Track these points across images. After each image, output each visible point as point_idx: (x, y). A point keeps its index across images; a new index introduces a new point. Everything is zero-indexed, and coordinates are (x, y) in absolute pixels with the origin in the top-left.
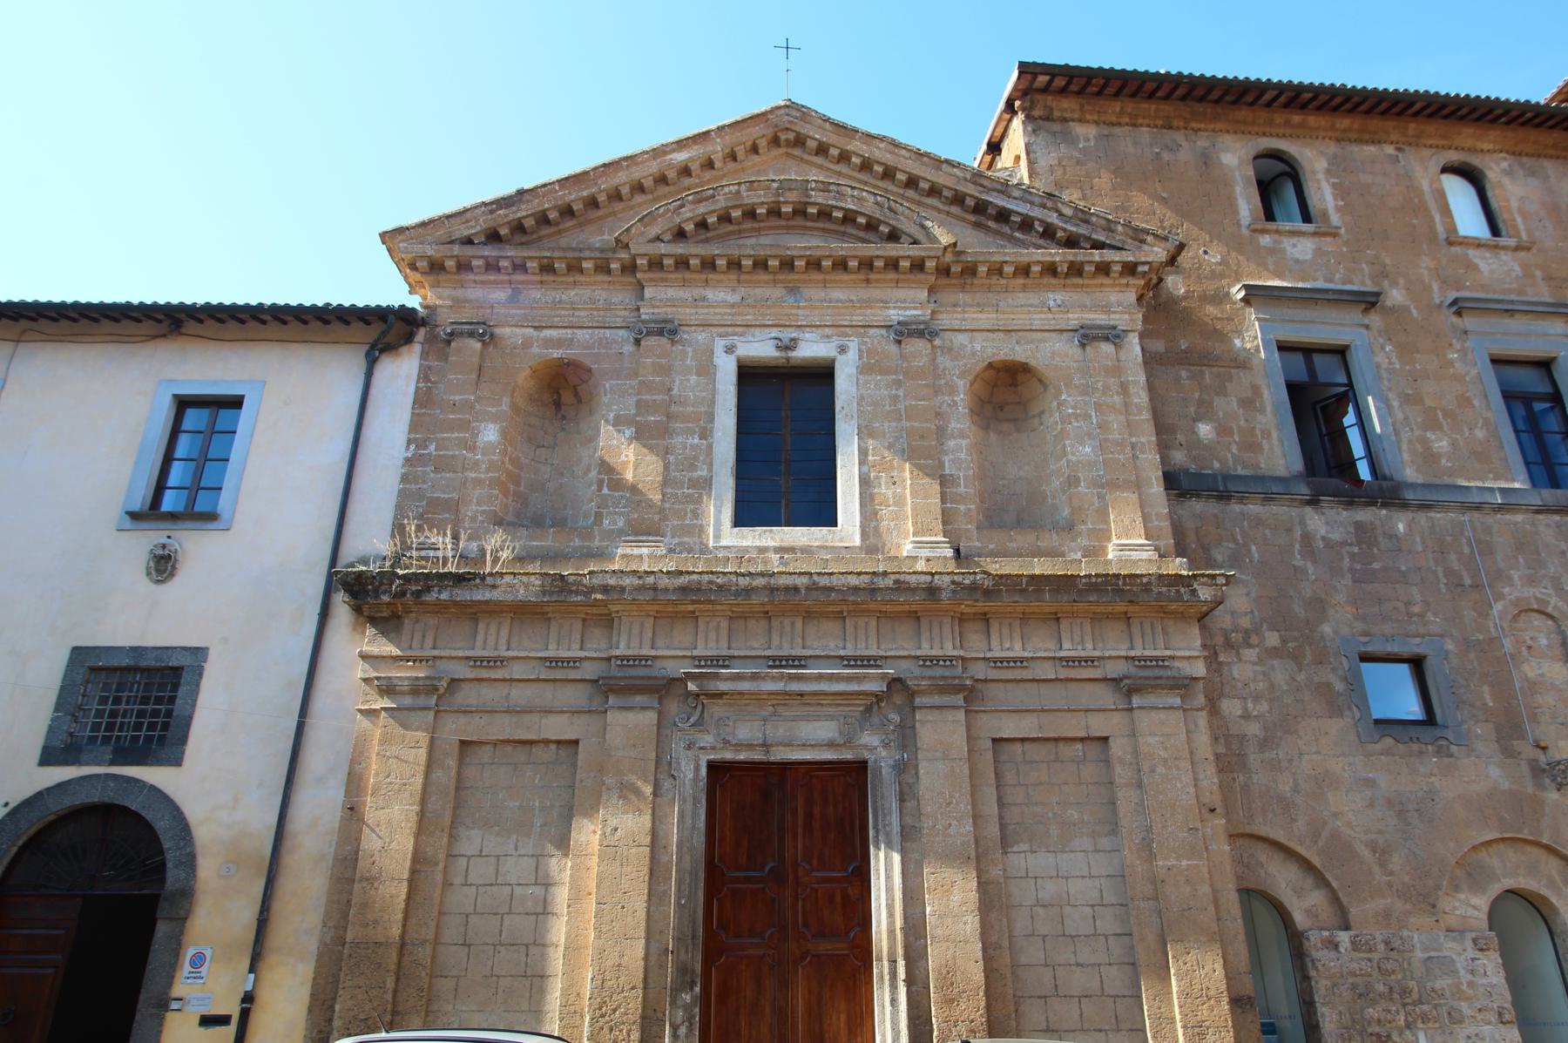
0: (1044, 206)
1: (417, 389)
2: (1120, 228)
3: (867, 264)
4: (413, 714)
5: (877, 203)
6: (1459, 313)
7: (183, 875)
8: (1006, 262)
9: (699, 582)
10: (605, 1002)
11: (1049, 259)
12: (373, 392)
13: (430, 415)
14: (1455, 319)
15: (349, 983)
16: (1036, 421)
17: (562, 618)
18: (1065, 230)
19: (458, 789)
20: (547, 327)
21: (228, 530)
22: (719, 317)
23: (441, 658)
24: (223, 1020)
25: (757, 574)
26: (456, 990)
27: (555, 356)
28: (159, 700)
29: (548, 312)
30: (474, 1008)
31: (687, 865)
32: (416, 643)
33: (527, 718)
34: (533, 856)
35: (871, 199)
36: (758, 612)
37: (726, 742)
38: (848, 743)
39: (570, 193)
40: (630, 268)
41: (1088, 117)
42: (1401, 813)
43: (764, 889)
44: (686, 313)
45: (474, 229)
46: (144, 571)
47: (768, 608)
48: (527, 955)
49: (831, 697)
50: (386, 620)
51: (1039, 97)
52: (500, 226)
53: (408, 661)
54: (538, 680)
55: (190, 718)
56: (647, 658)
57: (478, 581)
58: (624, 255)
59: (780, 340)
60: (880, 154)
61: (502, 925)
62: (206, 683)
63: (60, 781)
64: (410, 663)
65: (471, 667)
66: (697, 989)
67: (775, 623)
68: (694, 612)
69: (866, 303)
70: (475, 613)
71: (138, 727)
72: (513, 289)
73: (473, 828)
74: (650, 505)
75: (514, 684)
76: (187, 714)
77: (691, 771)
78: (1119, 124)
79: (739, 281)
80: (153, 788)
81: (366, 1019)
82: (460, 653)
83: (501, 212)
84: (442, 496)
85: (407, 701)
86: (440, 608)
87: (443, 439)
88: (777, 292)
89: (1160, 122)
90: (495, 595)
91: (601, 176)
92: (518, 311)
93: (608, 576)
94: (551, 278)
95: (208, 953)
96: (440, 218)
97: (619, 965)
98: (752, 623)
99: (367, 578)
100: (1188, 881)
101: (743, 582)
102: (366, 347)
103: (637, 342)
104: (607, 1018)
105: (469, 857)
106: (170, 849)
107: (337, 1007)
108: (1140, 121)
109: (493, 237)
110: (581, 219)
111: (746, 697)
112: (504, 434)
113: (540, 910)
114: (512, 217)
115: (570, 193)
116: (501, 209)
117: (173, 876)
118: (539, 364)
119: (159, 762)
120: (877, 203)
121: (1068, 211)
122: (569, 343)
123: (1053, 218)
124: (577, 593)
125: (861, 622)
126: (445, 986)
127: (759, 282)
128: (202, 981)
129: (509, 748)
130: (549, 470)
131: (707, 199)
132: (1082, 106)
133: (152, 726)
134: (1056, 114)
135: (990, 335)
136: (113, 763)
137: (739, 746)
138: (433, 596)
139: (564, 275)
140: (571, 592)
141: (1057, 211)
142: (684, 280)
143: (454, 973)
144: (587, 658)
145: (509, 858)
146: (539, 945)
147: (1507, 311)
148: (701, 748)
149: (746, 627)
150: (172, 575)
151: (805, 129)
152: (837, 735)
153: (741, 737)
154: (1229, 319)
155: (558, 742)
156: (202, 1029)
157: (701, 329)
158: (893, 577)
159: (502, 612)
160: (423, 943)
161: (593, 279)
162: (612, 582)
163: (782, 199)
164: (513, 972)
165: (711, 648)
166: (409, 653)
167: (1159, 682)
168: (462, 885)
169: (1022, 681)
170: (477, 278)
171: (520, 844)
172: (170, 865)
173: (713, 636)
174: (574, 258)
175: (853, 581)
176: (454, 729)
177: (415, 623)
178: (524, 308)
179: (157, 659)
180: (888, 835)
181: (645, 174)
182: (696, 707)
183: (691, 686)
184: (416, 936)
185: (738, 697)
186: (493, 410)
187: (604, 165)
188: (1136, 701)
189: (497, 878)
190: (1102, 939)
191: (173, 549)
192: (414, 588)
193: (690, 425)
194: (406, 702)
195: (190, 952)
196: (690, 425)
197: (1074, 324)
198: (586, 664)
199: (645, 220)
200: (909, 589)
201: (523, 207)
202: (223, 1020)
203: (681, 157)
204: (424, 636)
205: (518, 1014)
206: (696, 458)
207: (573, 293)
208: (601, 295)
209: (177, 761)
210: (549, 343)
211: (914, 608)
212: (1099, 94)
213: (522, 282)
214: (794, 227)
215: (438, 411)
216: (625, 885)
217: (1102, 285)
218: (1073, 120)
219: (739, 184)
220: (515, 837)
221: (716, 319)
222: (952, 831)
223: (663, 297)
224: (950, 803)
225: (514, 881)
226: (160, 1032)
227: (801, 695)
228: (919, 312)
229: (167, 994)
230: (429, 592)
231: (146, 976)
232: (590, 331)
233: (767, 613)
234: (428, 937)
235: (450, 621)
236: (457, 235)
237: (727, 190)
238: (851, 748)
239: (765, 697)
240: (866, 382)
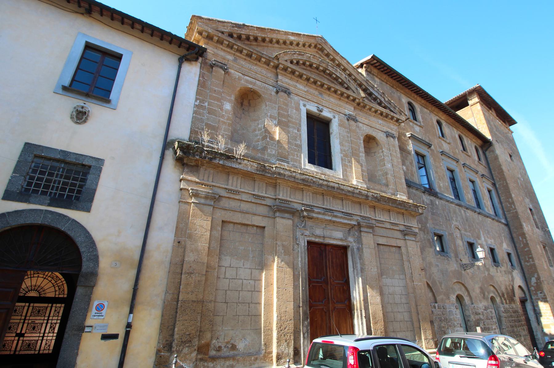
0: (381, 96)
1: (199, 80)
2: (397, 109)
3: (342, 94)
4: (205, 207)
5: (345, 77)
6: (442, 155)
7: (92, 265)
8: (373, 107)
9: (308, 179)
10: (282, 325)
11: (382, 110)
12: (181, 74)
13: (205, 92)
14: (441, 156)
15: (181, 319)
16: (373, 154)
17: (259, 181)
18: (384, 104)
19: (221, 239)
20: (246, 76)
21: (115, 109)
22: (301, 94)
23: (215, 186)
24: (115, 336)
25: (325, 180)
26: (223, 321)
27: (250, 87)
28: (75, 179)
29: (248, 70)
30: (230, 328)
31: (304, 276)
32: (205, 178)
33: (247, 215)
34: (250, 268)
36: (320, 193)
37: (313, 234)
38: (346, 240)
39: (259, 33)
40: (276, 67)
41: (379, 77)
42: (443, 274)
43: (322, 286)
44: (292, 89)
45: (227, 30)
46: (69, 116)
47: (324, 192)
48: (249, 307)
49: (341, 224)
50: (192, 166)
51: (370, 66)
52: (234, 33)
53: (202, 185)
54: (251, 202)
55: (95, 190)
56: (289, 201)
57: (235, 160)
58: (276, 62)
59: (319, 108)
60: (343, 63)
61: (239, 295)
62: (103, 175)
63: (17, 209)
64: (203, 186)
65: (227, 192)
66: (309, 320)
67: (325, 197)
68: (302, 188)
69: (340, 106)
70: (229, 172)
71: (63, 189)
72: (235, 57)
73: (227, 256)
74: (285, 149)
75: (242, 202)
76: (93, 188)
77: (303, 243)
78: (384, 81)
80: (74, 220)
81: (190, 334)
82: (223, 186)
83: (236, 28)
84: (212, 124)
85: (203, 201)
86: (217, 166)
87: (211, 102)
88: (316, 93)
89: (391, 85)
90: (240, 167)
91: (269, 32)
92: (237, 66)
93: (281, 169)
94: (249, 59)
95: (106, 304)
96: (216, 20)
97: (286, 311)
98: (318, 196)
99: (192, 147)
100: (420, 289)
101: (321, 182)
102: (179, 57)
103: (277, 92)
104: (283, 331)
105: (226, 267)
106: (84, 252)
107: (176, 329)
108: (388, 83)
109: (231, 35)
110: (258, 44)
111: (319, 220)
112: (234, 108)
113: (253, 290)
114: (239, 32)
115: (259, 33)
116: (236, 27)
117: (86, 266)
118: (243, 87)
119: (77, 209)
120: (345, 77)
121: (387, 99)
122: (254, 84)
123: (383, 100)
124: (268, 173)
125: (347, 202)
126: (218, 319)
127: (312, 87)
128: (103, 317)
129: (239, 226)
130: (239, 126)
131: (302, 55)
132: (378, 73)
133: (71, 191)
134: (372, 72)
135: (367, 126)
136: (49, 205)
137: (317, 236)
138: (217, 161)
139: (253, 60)
140: (266, 172)
141: (384, 98)
143: (221, 314)
144: (268, 197)
145: (241, 269)
146: (253, 303)
147: (449, 157)
148: (305, 235)
149: (317, 197)
150: (85, 122)
151: (325, 47)
152: (343, 237)
153: (317, 233)
154: (406, 141)
155: (257, 226)
156: (103, 341)
157: (296, 95)
158: (359, 190)
159: (238, 174)
160: (211, 301)
161: (262, 65)
162: (282, 172)
163: (321, 65)
164: (244, 314)
165: (308, 202)
166: (203, 182)
167: (412, 233)
168: (224, 278)
169: (383, 227)
170: (223, 48)
171: (245, 264)
172: (84, 260)
173: (308, 197)
174: (260, 56)
175: (349, 189)
176: (220, 215)
177: (206, 170)
178: (240, 66)
179: (76, 159)
180: (357, 270)
181: (281, 38)
182: (303, 221)
183: (305, 214)
184: (208, 299)
185: (316, 220)
186: (229, 98)
187: (271, 29)
188: (407, 237)
189: (237, 277)
190: (403, 304)
191: (87, 110)
192: (209, 156)
193: (294, 126)
194: (202, 201)
195: (96, 303)
196: (294, 126)
197: (385, 130)
198: (268, 199)
199: (285, 53)
200: (362, 195)
201: (244, 30)
202: (115, 336)
203: (292, 38)
204: (209, 177)
205: (247, 331)
206: (296, 137)
207: (255, 68)
208: (264, 72)
209: (88, 209)
210: (247, 81)
211: (360, 201)
212: (382, 71)
213: (239, 57)
214: (321, 75)
215: (208, 91)
216: (286, 282)
217: (390, 122)
218: (375, 76)
219: (311, 55)
220: (243, 261)
221: (300, 94)
222: (372, 270)
223: (285, 80)
224: (371, 262)
225: (243, 278)
226: (79, 344)
227: (334, 222)
228: (352, 113)
229: (83, 324)
230: (215, 159)
231: (70, 315)
232: (261, 83)
233: (323, 193)
234: (213, 299)
235: (218, 172)
236: (220, 29)
237: (307, 55)
238: (346, 241)
239: (324, 221)
240: (341, 129)
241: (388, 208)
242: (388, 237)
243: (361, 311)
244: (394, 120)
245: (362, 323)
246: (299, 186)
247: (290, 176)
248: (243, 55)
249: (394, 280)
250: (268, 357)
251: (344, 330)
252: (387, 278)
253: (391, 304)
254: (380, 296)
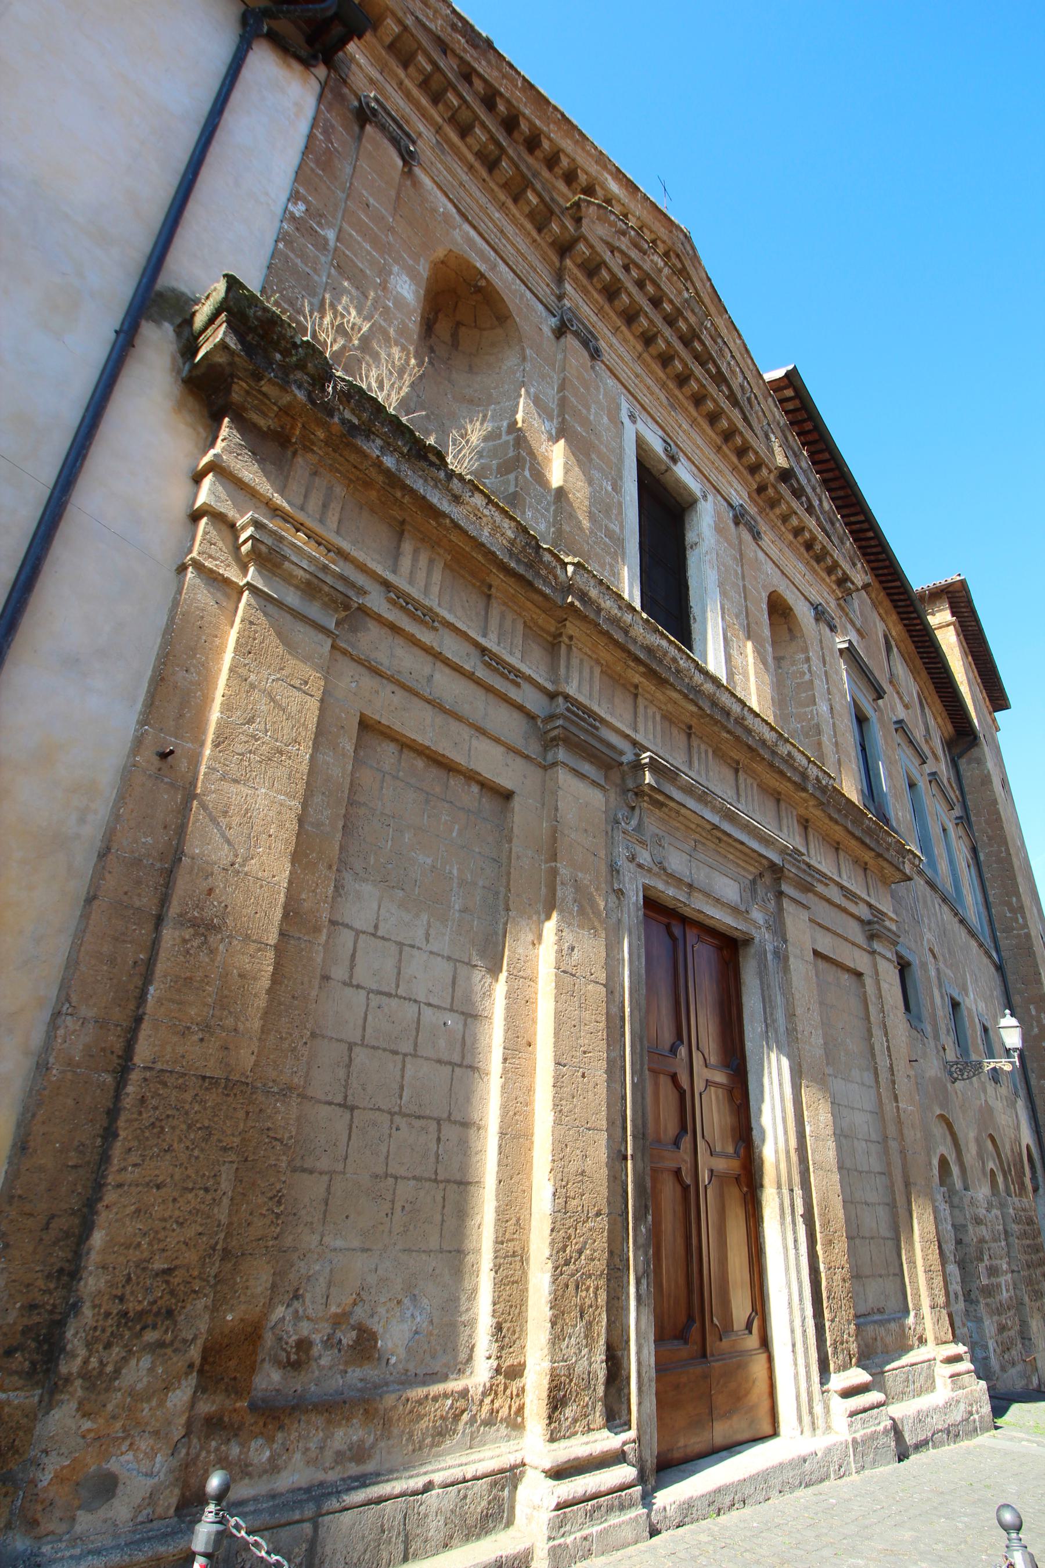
1: (311, 137)
13: (329, 188)
27: (478, 265)
30: (356, 1243)
33: (454, 726)
35: (740, 379)
48: (439, 1140)
49: (738, 854)
57: (442, 475)
61: (403, 1077)
68: (636, 687)
74: (581, 529)
79: (640, 356)
81: (168, 1271)
82: (379, 570)
85: (292, 598)
97: (583, 1173)
99: (282, 336)
101: (698, 678)
105: (358, 933)
107: (98, 1238)
111: (681, 818)
113: (456, 1058)
116: (464, 37)
126: (312, 1189)
129: (420, 763)
138: (373, 448)
140: (538, 574)
141: (820, 500)
142: (602, 308)
143: (324, 1164)
145: (415, 952)
146: (455, 1122)
153: (674, 867)
158: (789, 747)
162: (594, 593)
166: (301, 516)
168: (344, 984)
170: (407, 83)
171: (432, 932)
173: (650, 724)
177: (315, 473)
180: (776, 1031)
184: (273, 1074)
185: (673, 815)
186: (411, 262)
187: (563, 115)
189: (398, 986)
192: (348, 415)
203: (614, 187)
205: (424, 1257)
220: (425, 917)
221: (623, 376)
225: (421, 998)
239: (693, 826)
241: (837, 837)
244: (833, 578)
246: (630, 673)
247: (615, 621)
248: (469, 148)
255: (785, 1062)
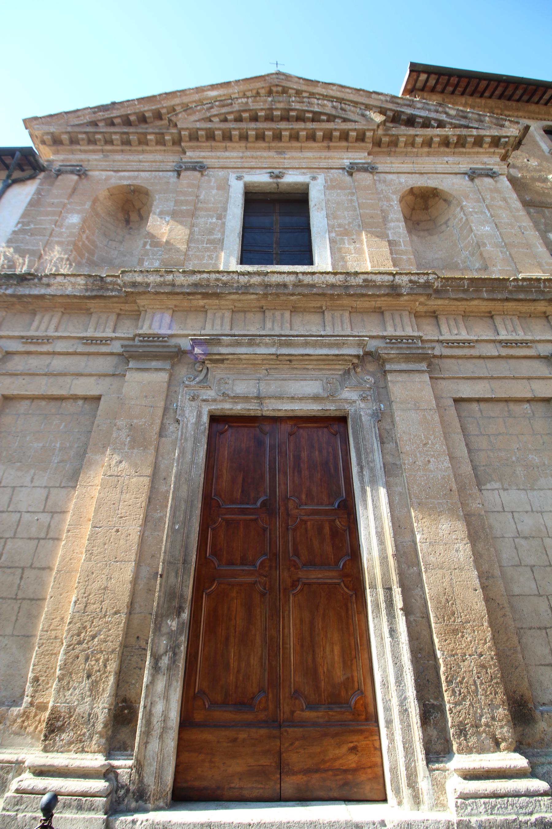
0: (437, 111)
5: (333, 107)
8: (417, 135)
9: (208, 280)
10: (85, 628)
16: (444, 227)
31: (184, 493)
33: (61, 379)
34: (45, 487)
35: (329, 104)
36: (255, 307)
38: (331, 397)
43: (255, 520)
48: (21, 578)
49: (315, 363)
52: (98, 120)
58: (174, 131)
66: (185, 615)
68: (204, 307)
74: (178, 250)
75: (56, 356)
79: (246, 148)
82: (16, 334)
91: (164, 100)
93: (136, 275)
94: (127, 148)
97: (105, 588)
98: (250, 315)
104: (85, 645)
111: (244, 362)
114: (107, 116)
116: (101, 111)
120: (333, 107)
125: (337, 314)
129: (43, 403)
131: (228, 105)
137: (236, 398)
142: (211, 146)
145: (23, 489)
148: (204, 401)
152: (321, 391)
153: (238, 391)
158: (362, 277)
163: (274, 107)
170: (82, 148)
171: (36, 477)
173: (218, 322)
180: (372, 470)
185: (237, 362)
187: (166, 94)
189: (9, 506)
200: (375, 286)
206: (213, 229)
210: (121, 178)
211: (379, 304)
212: (453, 93)
213: (110, 151)
216: (122, 511)
217: (478, 153)
222: (431, 466)
224: (425, 444)
225: (24, 509)
232: (149, 173)
238: (334, 401)
239: (260, 362)
241: (483, 309)
242: (492, 378)
243: (390, 589)
244: (486, 146)
245: (393, 632)
246: (195, 303)
247: (161, 284)
248: (117, 145)
249: (535, 493)
250: (37, 718)
251: (332, 651)
252: (504, 490)
253: (532, 567)
254: (466, 540)
255: (383, 492)
